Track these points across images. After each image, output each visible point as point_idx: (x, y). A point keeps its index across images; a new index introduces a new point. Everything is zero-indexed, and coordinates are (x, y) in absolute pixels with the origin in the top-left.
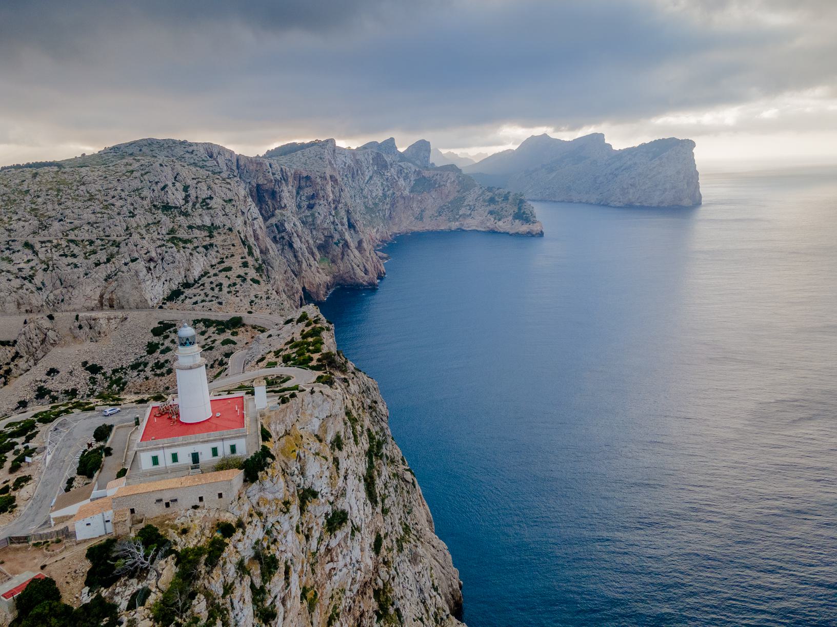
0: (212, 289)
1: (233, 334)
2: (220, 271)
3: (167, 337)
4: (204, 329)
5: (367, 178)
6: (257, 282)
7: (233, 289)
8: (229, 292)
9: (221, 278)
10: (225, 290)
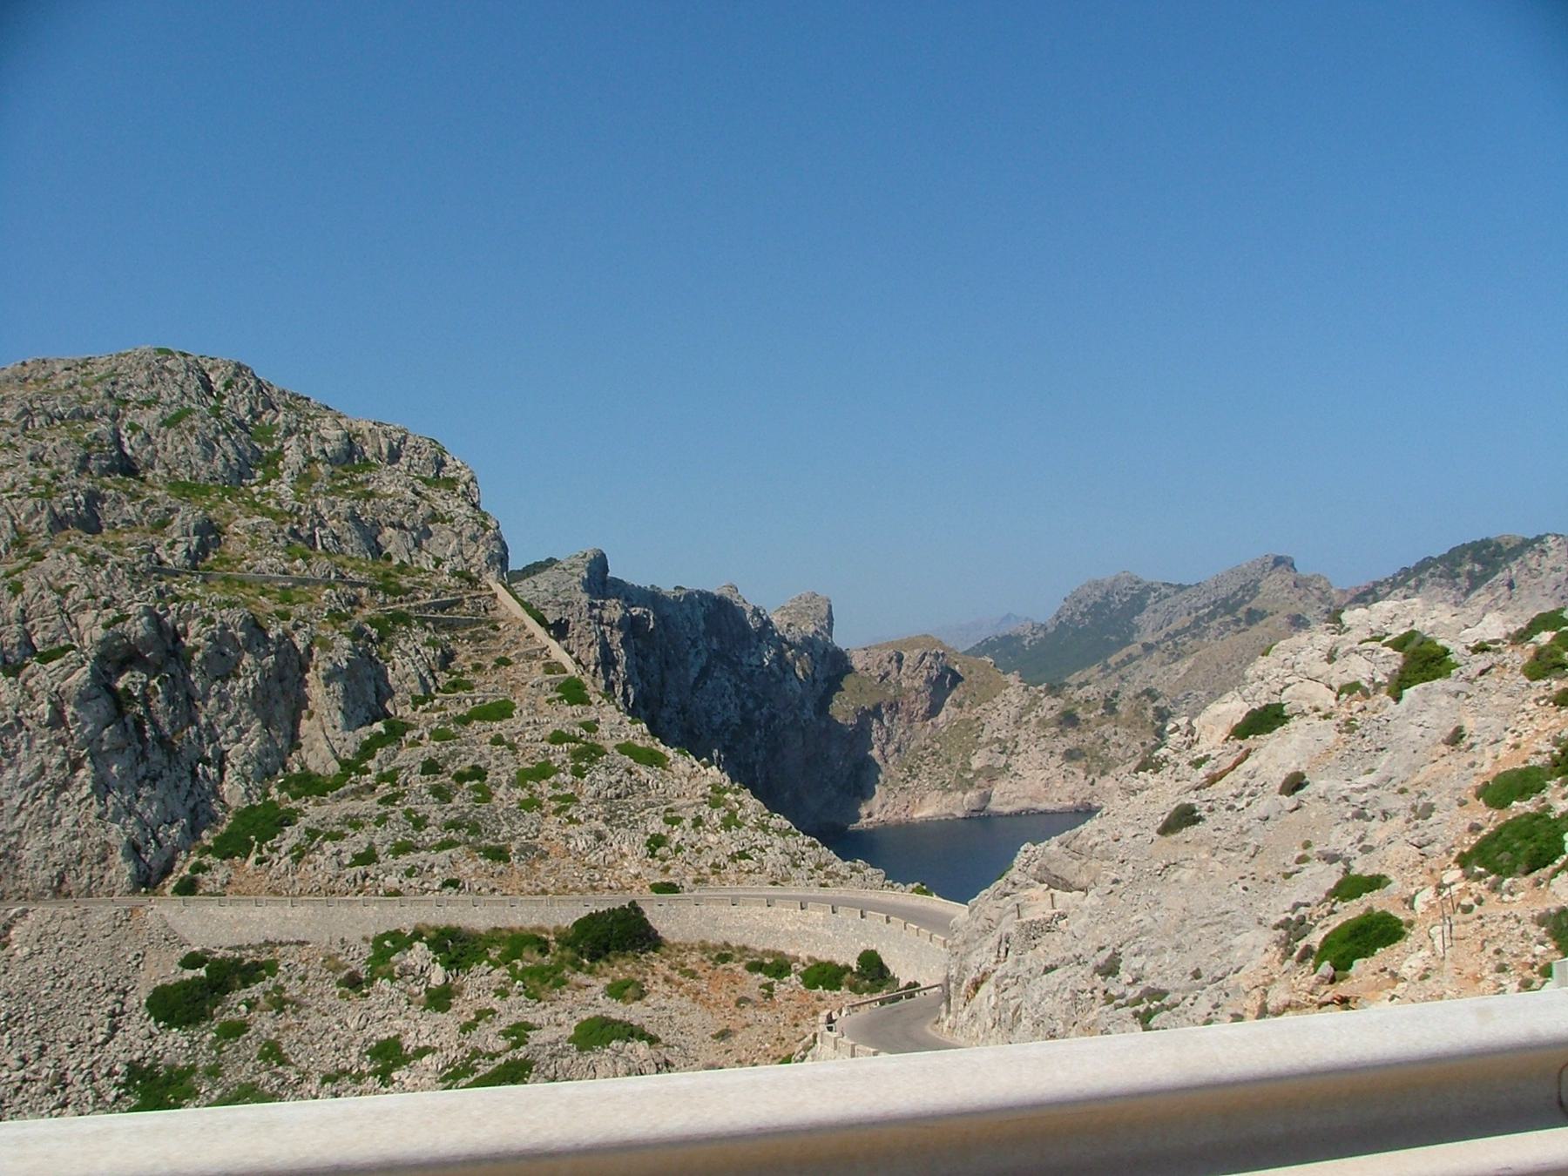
0: (442, 794)
1: (618, 991)
2: (464, 721)
3: (236, 1030)
4: (437, 976)
5: (694, 673)
6: (654, 760)
7: (544, 788)
8: (530, 804)
9: (477, 746)
10: (506, 797)
